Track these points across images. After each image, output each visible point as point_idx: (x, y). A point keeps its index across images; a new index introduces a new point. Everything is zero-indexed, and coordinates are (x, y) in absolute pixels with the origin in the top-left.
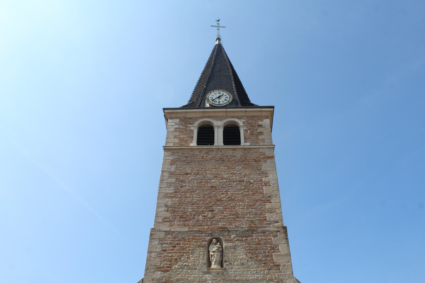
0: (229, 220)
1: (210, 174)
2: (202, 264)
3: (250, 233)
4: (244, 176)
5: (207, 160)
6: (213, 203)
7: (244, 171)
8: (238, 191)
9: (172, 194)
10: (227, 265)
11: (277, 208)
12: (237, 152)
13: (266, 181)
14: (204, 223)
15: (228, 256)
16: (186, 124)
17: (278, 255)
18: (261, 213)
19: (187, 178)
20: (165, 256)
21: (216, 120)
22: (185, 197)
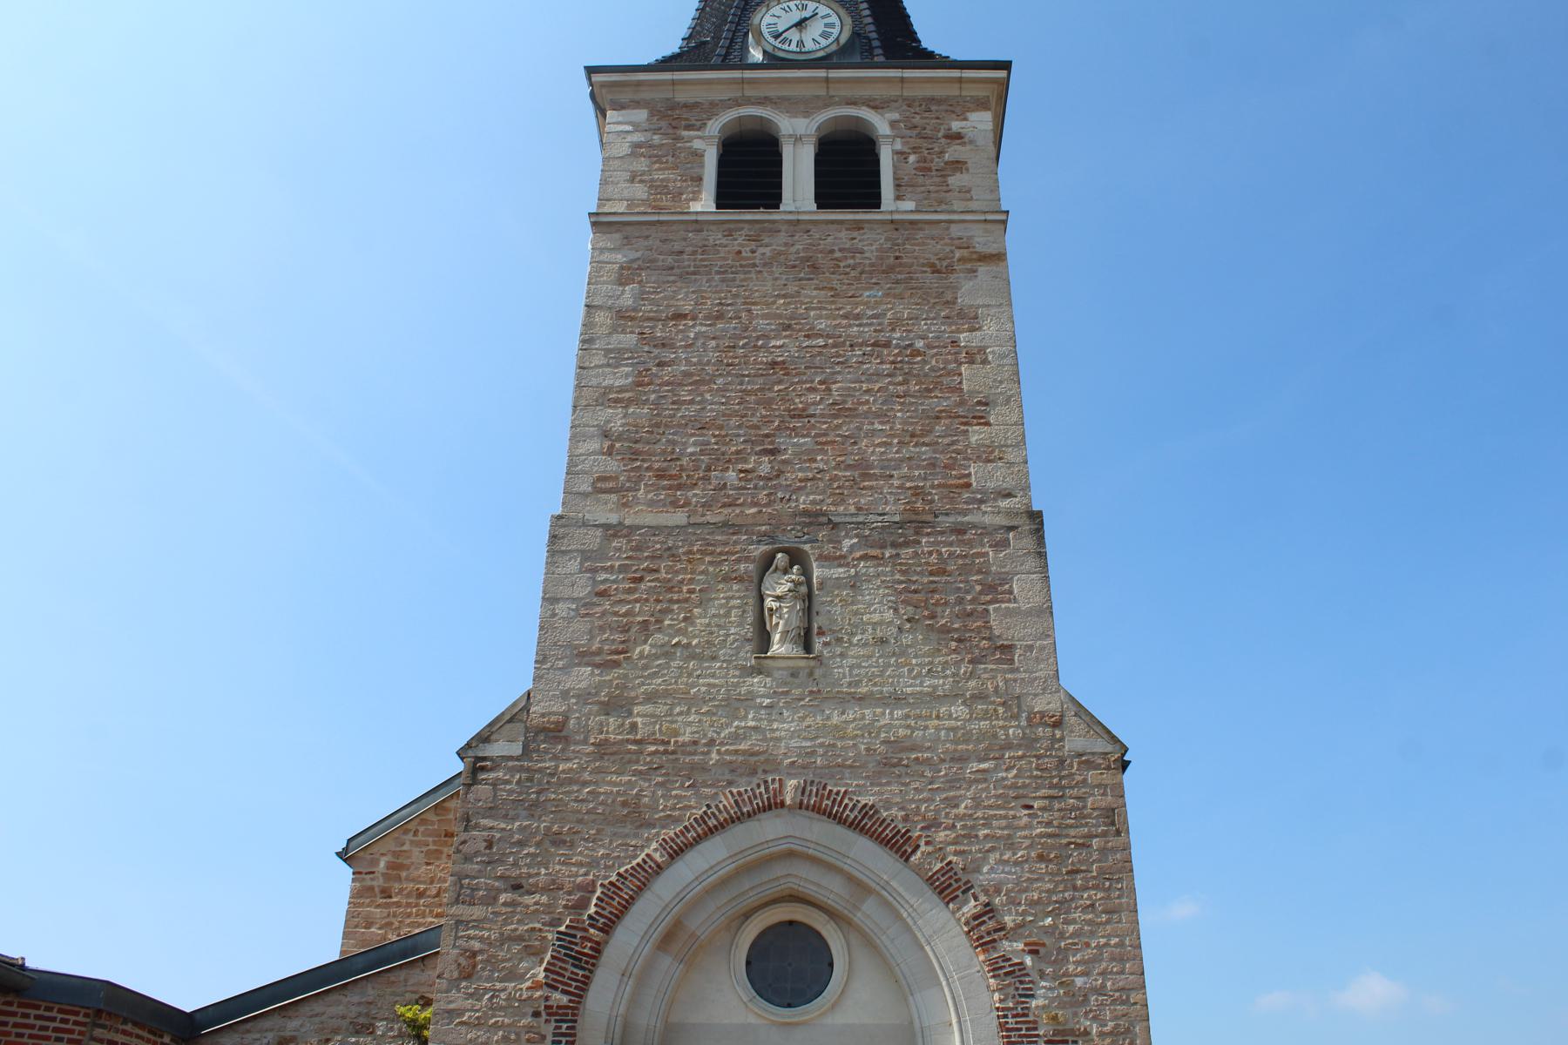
0: (835, 486)
1: (765, 316)
2: (737, 640)
3: (912, 531)
4: (890, 324)
5: (754, 265)
6: (776, 424)
7: (892, 309)
8: (868, 381)
9: (627, 391)
10: (826, 644)
11: (1011, 446)
12: (866, 237)
13: (974, 344)
14: (743, 494)
15: (830, 612)
17: (1009, 613)
18: (950, 462)
19: (682, 331)
20: (604, 614)
22: (674, 403)
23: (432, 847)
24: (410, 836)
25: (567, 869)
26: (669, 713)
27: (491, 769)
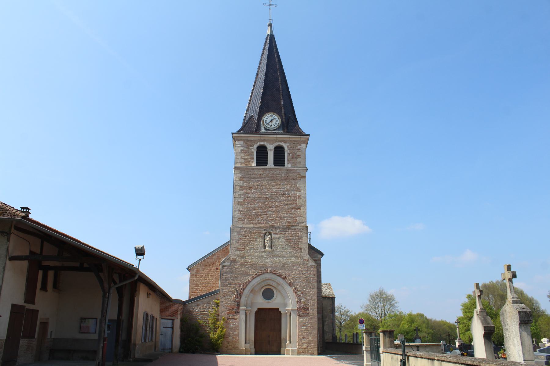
1: (265, 188)
5: (263, 177)
8: (282, 201)
17: (302, 243)
20: (241, 242)
22: (250, 205)
23: (203, 267)
24: (199, 266)
25: (237, 281)
26: (251, 258)
27: (225, 267)
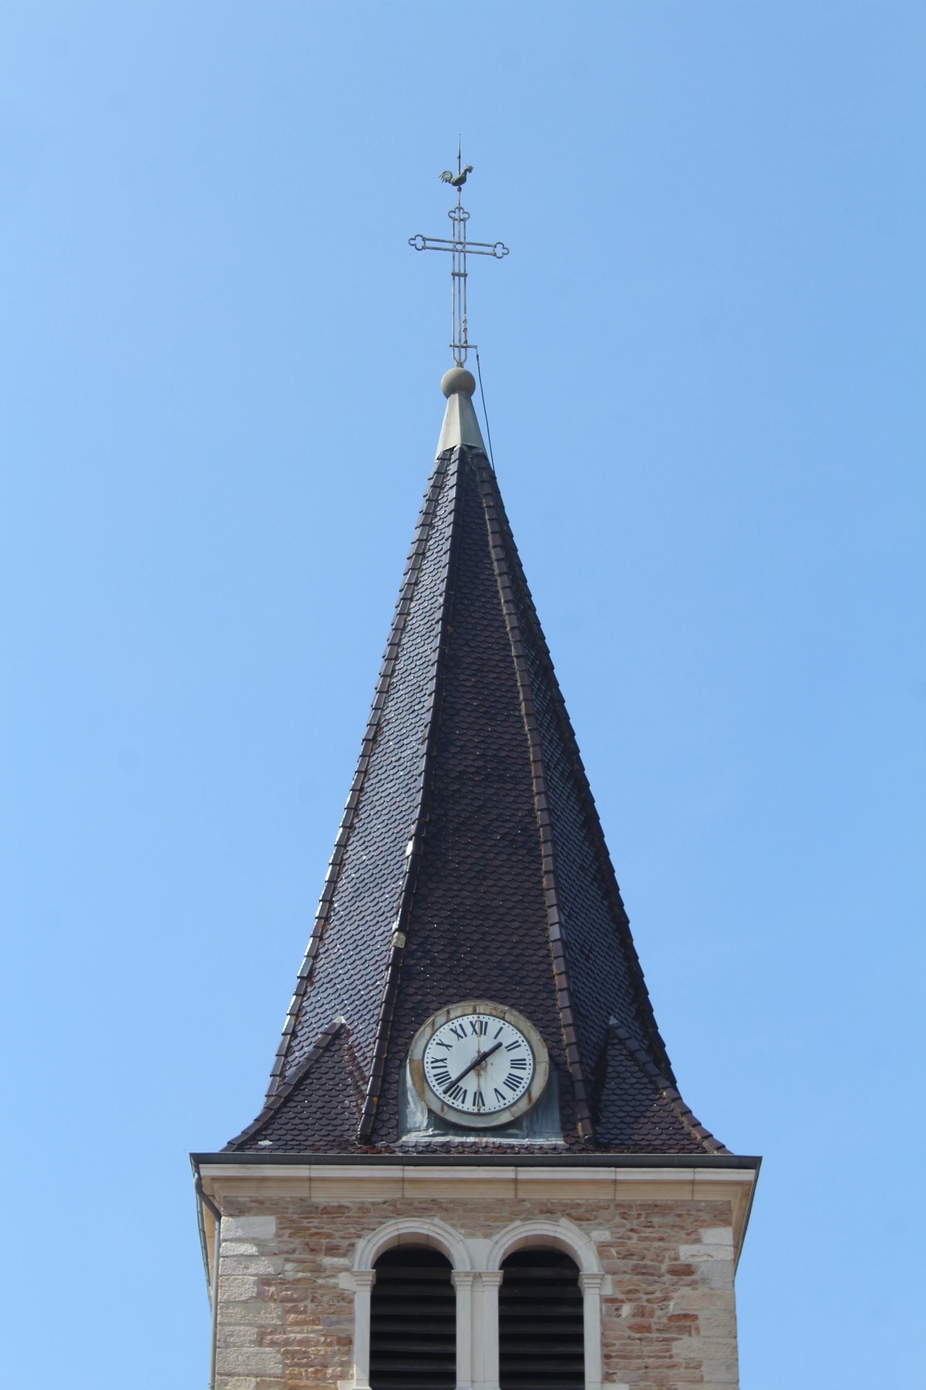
16: (313, 1250)
21: (462, 1226)
